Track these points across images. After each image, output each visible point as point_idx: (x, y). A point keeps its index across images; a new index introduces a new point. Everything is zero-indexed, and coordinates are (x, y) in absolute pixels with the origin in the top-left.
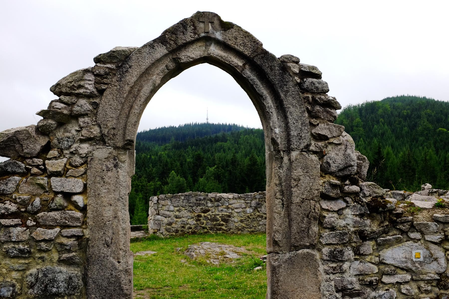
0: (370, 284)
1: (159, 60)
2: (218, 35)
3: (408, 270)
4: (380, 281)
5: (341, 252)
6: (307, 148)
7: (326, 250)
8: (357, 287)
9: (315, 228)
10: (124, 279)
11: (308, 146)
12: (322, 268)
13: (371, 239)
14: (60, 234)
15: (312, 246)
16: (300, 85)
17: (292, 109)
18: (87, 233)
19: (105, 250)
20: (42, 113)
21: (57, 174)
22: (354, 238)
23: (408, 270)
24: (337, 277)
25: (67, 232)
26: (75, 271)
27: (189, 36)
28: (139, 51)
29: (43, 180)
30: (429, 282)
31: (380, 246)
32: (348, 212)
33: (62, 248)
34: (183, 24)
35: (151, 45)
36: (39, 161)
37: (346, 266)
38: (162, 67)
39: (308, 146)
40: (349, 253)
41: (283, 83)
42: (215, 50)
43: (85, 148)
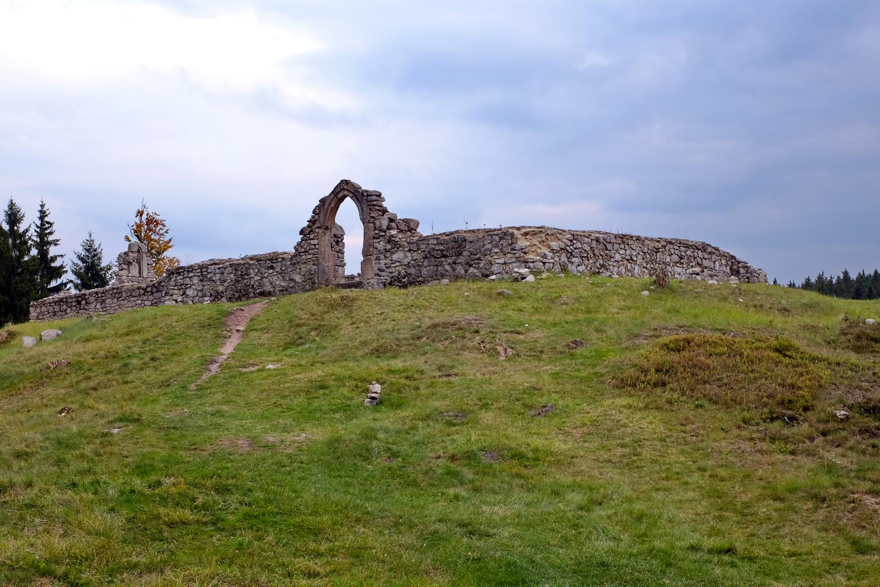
0: (387, 267)
1: (333, 199)
2: (346, 187)
3: (399, 262)
4: (390, 266)
5: (379, 257)
6: (369, 222)
7: (375, 256)
8: (384, 268)
9: (371, 249)
10: (326, 269)
11: (369, 221)
12: (374, 262)
13: (389, 251)
14: (313, 257)
15: (371, 255)
16: (367, 200)
17: (364, 209)
18: (318, 256)
19: (322, 261)
20: (308, 221)
21: (312, 239)
22: (383, 251)
23: (399, 262)
24: (379, 265)
25: (315, 256)
26: (316, 267)
27: (339, 190)
28: (327, 197)
29: (309, 241)
30: (405, 265)
31: (392, 253)
32: (381, 243)
33: (313, 261)
34: (337, 186)
35: (330, 195)
36: (308, 236)
37: (381, 261)
38: (334, 201)
39: (369, 221)
40: (382, 257)
41: (362, 200)
42: (346, 193)
43: (317, 230)
